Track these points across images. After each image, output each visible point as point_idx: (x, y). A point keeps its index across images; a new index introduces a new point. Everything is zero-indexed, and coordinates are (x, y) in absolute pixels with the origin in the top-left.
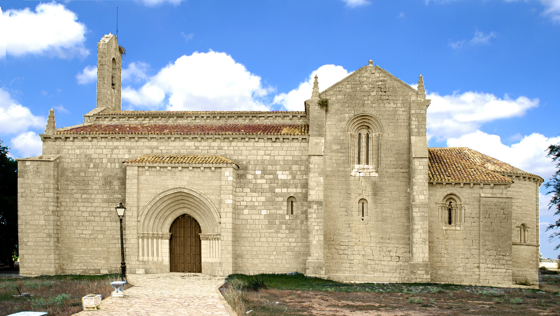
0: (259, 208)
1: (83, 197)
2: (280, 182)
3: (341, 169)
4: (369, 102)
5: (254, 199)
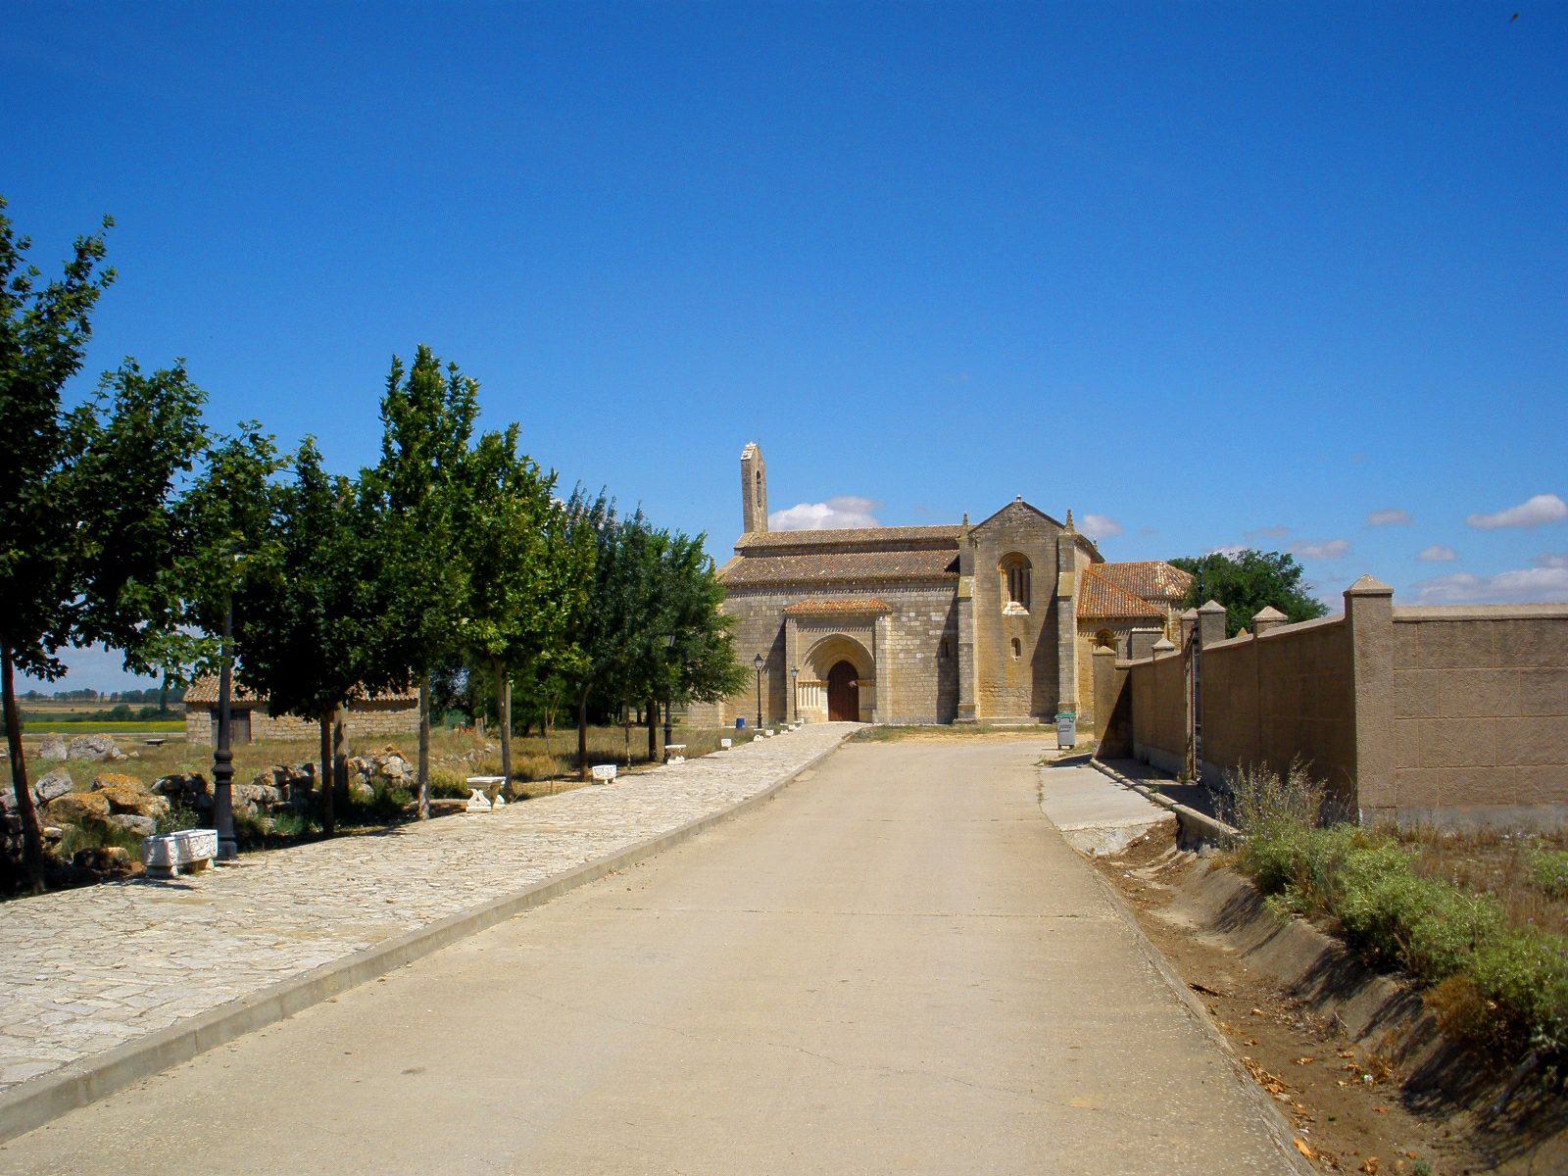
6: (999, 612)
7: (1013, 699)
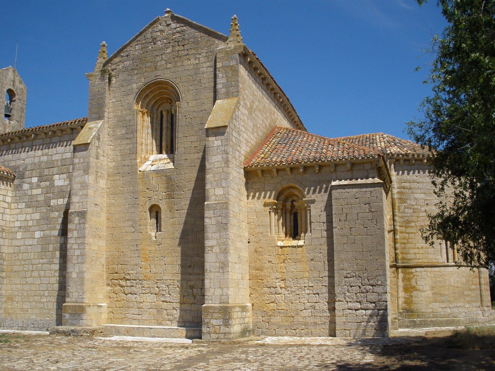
0: (33, 229)
2: (56, 191)
3: (127, 162)
4: (163, 62)
5: (28, 218)
6: (132, 170)
7: (150, 298)
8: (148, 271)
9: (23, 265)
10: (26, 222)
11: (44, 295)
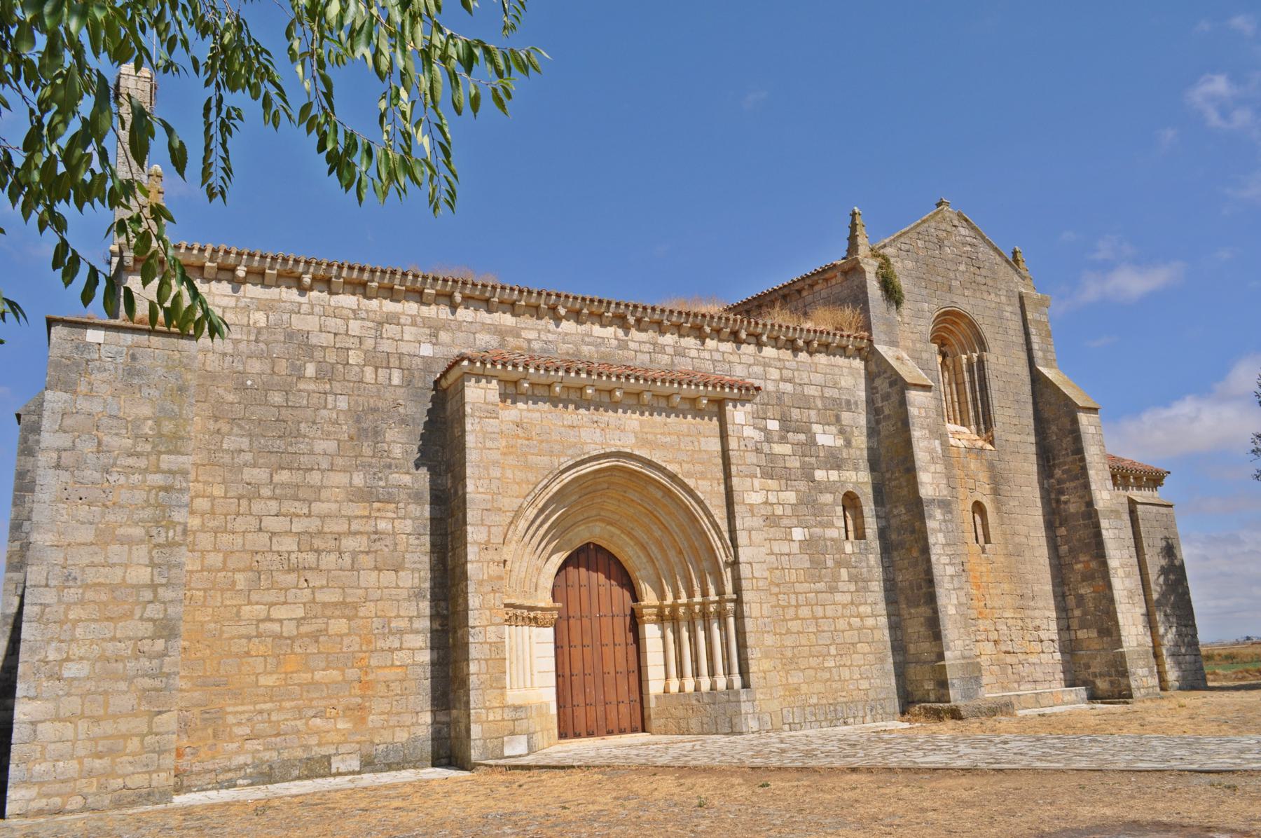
0: (785, 522)
1: (276, 478)
2: (822, 454)
5: (772, 499)
8: (982, 604)
9: (777, 595)
10: (769, 508)
11: (829, 654)
